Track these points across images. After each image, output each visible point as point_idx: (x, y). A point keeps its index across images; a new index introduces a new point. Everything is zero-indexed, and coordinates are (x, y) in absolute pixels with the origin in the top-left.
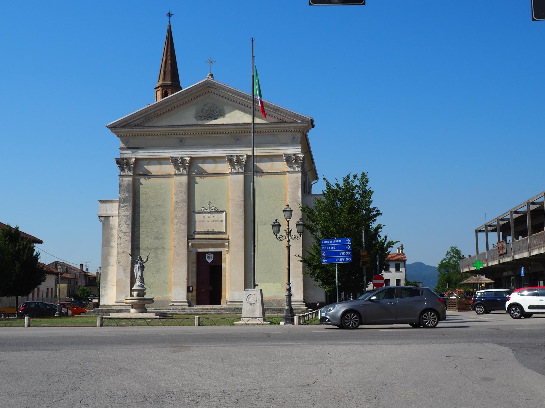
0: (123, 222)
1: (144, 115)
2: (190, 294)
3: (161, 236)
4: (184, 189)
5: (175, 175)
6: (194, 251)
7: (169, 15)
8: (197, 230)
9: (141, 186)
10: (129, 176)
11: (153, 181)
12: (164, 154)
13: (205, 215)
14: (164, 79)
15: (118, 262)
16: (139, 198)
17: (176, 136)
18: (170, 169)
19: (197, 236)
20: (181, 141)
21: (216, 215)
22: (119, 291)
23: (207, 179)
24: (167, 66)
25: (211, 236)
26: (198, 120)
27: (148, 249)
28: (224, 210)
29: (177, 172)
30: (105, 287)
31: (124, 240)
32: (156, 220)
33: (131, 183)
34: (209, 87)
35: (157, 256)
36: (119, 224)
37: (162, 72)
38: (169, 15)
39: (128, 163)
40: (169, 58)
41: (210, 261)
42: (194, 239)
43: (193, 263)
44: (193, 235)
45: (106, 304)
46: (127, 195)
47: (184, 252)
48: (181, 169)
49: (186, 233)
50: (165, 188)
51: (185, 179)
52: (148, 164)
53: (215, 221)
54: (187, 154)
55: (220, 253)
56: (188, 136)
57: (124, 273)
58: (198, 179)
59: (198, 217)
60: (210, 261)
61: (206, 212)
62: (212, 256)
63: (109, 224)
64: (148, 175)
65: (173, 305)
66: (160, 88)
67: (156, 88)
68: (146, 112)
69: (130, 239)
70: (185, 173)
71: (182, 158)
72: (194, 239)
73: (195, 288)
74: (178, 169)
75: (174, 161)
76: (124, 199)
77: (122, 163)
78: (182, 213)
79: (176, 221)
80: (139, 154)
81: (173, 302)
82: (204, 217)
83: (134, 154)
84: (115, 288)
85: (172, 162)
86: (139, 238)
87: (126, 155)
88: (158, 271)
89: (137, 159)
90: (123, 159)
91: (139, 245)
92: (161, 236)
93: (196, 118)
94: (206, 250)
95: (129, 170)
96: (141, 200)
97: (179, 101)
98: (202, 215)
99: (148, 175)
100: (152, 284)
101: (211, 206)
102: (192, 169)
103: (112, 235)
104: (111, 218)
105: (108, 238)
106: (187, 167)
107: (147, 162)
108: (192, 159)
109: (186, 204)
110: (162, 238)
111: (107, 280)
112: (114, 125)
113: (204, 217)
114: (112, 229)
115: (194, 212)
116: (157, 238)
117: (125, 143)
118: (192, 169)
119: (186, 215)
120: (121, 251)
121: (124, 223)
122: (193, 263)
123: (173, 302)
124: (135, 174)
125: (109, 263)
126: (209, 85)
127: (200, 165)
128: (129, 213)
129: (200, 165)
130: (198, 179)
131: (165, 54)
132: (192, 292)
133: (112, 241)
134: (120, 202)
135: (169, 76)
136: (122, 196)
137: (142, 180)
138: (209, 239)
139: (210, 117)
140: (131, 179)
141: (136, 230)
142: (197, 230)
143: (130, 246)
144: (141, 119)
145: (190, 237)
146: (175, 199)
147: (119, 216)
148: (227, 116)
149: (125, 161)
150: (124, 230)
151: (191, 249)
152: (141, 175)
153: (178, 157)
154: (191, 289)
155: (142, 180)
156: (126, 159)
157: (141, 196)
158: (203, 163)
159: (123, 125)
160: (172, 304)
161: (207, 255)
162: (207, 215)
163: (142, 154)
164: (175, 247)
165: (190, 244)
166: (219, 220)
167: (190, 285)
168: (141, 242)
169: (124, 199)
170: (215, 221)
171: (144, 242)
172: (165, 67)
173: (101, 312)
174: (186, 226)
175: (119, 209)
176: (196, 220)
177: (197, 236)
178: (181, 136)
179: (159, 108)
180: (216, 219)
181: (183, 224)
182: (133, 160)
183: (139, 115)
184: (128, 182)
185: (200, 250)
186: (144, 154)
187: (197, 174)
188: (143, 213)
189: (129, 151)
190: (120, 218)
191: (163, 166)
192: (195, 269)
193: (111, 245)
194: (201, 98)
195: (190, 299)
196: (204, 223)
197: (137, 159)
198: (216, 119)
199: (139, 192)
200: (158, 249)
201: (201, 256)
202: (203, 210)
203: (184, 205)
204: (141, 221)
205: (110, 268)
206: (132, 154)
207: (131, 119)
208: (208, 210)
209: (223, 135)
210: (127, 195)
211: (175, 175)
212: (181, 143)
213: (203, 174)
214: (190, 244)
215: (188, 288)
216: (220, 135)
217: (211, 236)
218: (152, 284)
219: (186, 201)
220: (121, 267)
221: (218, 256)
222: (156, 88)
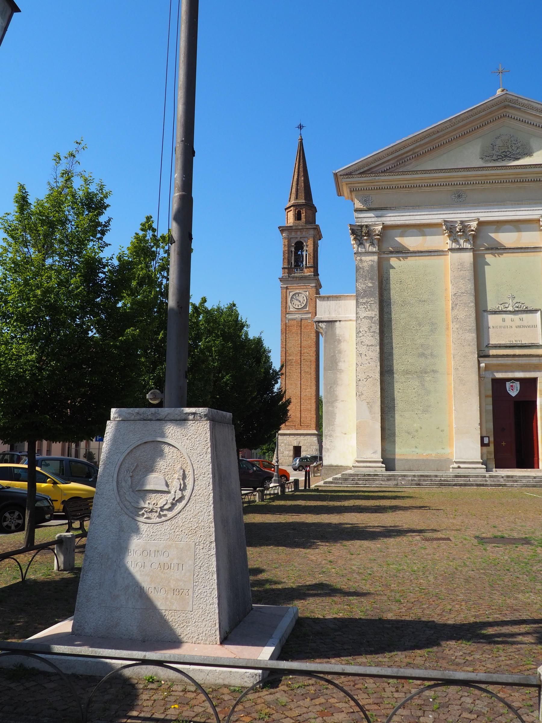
0: (364, 328)
1: (397, 154)
2: (485, 449)
3: (429, 351)
4: (469, 274)
5: (451, 250)
6: (489, 376)
7: (301, 127)
8: (493, 341)
9: (391, 271)
10: (373, 253)
11: (411, 261)
12: (430, 217)
13: (504, 316)
14: (297, 198)
15: (359, 395)
16: (389, 289)
17: (449, 188)
18: (443, 242)
19: (492, 352)
20: (459, 196)
21: (524, 316)
22: (361, 443)
23: (507, 257)
24: (300, 183)
25: (518, 352)
26: (486, 161)
27: (407, 372)
28: (538, 308)
29: (454, 246)
30: (331, 436)
31: (368, 358)
32: (420, 324)
33: (376, 265)
34: (505, 107)
35: (423, 385)
36: (358, 332)
37: (294, 190)
38: (301, 127)
39: (369, 234)
40: (302, 174)
41: (514, 394)
42: (488, 356)
43: (487, 396)
44: (486, 349)
45: (334, 463)
46: (370, 285)
47: (474, 377)
48: (461, 241)
49: (475, 347)
50: (435, 273)
51: (468, 257)
52: (402, 235)
53: (524, 327)
54: (472, 216)
55: (535, 380)
56: (470, 187)
57: (370, 412)
58: (489, 258)
59: (493, 320)
60: (514, 394)
61: (506, 312)
62: (517, 385)
63: (334, 334)
64: (402, 252)
65: (459, 467)
66: (292, 208)
67: (286, 209)
68: (400, 149)
69: (378, 356)
70: (469, 246)
71: (462, 222)
72: (488, 356)
73: (492, 439)
74: (455, 241)
75: (451, 229)
76: (365, 291)
77: (360, 233)
78: (467, 313)
79: (457, 326)
80: (388, 219)
81: (456, 462)
82: (504, 320)
83: (380, 219)
84: (354, 435)
85: (447, 229)
86: (391, 354)
87: (365, 220)
88: (425, 411)
89: (385, 228)
90: (362, 226)
91: (392, 366)
92: (429, 351)
93: (482, 158)
94: (510, 375)
95: (372, 244)
96: (392, 292)
97: (456, 130)
98: (499, 317)
99: (402, 252)
100: (417, 431)
101: (515, 301)
102: (479, 242)
103: (340, 352)
104: (338, 323)
105: (334, 356)
106: (471, 238)
107: (399, 231)
108: (481, 224)
109: (472, 298)
110: (432, 355)
111: (333, 425)
112: (348, 171)
113: (504, 320)
114: (339, 341)
115: (485, 311)
116: (423, 355)
117: (364, 201)
118: (479, 242)
119: (474, 315)
120: (362, 376)
121: (366, 329)
122: (487, 396)
123: (456, 462)
124: (380, 253)
125: (337, 396)
126: (507, 103)
127: (492, 235)
128: (375, 313)
129: (492, 235)
130: (489, 258)
131: (296, 170)
132: (488, 445)
133: (339, 361)
134: (357, 297)
135: (302, 194)
136: (361, 286)
137: (394, 261)
138: (514, 356)
139: (506, 156)
140: (375, 258)
141: (386, 341)
142: (493, 342)
143: (379, 367)
144: (392, 162)
145: (482, 355)
146: (451, 290)
147: (357, 318)
148: (535, 154)
149: (364, 230)
150: (367, 342)
151: (483, 373)
152: (391, 252)
153: (456, 222)
154: (486, 441)
155: (394, 261)
156: (367, 226)
157: (392, 286)
158: (496, 231)
159: (362, 171)
160: (456, 465)
161: (508, 384)
162: (508, 317)
163: (393, 218)
164: (456, 369)
165: (483, 365)
166: (530, 324)
167: (484, 434)
168: (395, 361)
169: (365, 291)
170: (524, 327)
171: (400, 362)
172: (297, 184)
173: (359, 480)
174: (474, 335)
175: (357, 306)
176: (490, 325)
177: (492, 352)
178: (459, 188)
179: (422, 142)
180: (525, 323)
181: (470, 331)
182: (380, 228)
183: (388, 155)
184: (370, 263)
185: (499, 375)
186: (396, 218)
187: (487, 249)
188: (398, 315)
189: (371, 215)
190: (359, 321)
191: (428, 238)
192: (490, 407)
193: (339, 368)
194: (491, 125)
195: (485, 458)
196: (503, 330)
197: (385, 228)
198: (518, 159)
199: (388, 279)
200: (426, 373)
201: (499, 385)
202: (501, 308)
203: (470, 300)
204: (393, 327)
205: (339, 405)
206: (376, 219)
207: (375, 161)
208: (510, 309)
209: (532, 185)
210: (370, 285)
211: (451, 250)
212: (459, 199)
213: (498, 249)
214: (483, 365)
215: (482, 438)
216: (526, 185)
217: (518, 352)
218: (417, 431)
219: (473, 292)
220: (365, 404)
221: (529, 385)
222: (286, 209)
